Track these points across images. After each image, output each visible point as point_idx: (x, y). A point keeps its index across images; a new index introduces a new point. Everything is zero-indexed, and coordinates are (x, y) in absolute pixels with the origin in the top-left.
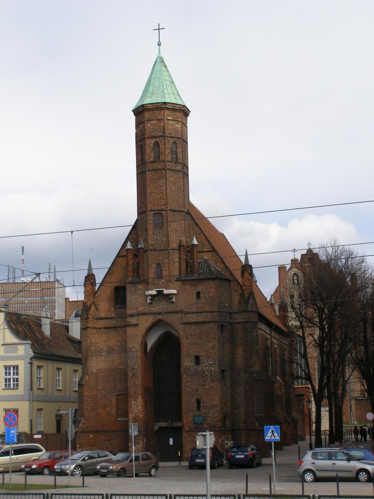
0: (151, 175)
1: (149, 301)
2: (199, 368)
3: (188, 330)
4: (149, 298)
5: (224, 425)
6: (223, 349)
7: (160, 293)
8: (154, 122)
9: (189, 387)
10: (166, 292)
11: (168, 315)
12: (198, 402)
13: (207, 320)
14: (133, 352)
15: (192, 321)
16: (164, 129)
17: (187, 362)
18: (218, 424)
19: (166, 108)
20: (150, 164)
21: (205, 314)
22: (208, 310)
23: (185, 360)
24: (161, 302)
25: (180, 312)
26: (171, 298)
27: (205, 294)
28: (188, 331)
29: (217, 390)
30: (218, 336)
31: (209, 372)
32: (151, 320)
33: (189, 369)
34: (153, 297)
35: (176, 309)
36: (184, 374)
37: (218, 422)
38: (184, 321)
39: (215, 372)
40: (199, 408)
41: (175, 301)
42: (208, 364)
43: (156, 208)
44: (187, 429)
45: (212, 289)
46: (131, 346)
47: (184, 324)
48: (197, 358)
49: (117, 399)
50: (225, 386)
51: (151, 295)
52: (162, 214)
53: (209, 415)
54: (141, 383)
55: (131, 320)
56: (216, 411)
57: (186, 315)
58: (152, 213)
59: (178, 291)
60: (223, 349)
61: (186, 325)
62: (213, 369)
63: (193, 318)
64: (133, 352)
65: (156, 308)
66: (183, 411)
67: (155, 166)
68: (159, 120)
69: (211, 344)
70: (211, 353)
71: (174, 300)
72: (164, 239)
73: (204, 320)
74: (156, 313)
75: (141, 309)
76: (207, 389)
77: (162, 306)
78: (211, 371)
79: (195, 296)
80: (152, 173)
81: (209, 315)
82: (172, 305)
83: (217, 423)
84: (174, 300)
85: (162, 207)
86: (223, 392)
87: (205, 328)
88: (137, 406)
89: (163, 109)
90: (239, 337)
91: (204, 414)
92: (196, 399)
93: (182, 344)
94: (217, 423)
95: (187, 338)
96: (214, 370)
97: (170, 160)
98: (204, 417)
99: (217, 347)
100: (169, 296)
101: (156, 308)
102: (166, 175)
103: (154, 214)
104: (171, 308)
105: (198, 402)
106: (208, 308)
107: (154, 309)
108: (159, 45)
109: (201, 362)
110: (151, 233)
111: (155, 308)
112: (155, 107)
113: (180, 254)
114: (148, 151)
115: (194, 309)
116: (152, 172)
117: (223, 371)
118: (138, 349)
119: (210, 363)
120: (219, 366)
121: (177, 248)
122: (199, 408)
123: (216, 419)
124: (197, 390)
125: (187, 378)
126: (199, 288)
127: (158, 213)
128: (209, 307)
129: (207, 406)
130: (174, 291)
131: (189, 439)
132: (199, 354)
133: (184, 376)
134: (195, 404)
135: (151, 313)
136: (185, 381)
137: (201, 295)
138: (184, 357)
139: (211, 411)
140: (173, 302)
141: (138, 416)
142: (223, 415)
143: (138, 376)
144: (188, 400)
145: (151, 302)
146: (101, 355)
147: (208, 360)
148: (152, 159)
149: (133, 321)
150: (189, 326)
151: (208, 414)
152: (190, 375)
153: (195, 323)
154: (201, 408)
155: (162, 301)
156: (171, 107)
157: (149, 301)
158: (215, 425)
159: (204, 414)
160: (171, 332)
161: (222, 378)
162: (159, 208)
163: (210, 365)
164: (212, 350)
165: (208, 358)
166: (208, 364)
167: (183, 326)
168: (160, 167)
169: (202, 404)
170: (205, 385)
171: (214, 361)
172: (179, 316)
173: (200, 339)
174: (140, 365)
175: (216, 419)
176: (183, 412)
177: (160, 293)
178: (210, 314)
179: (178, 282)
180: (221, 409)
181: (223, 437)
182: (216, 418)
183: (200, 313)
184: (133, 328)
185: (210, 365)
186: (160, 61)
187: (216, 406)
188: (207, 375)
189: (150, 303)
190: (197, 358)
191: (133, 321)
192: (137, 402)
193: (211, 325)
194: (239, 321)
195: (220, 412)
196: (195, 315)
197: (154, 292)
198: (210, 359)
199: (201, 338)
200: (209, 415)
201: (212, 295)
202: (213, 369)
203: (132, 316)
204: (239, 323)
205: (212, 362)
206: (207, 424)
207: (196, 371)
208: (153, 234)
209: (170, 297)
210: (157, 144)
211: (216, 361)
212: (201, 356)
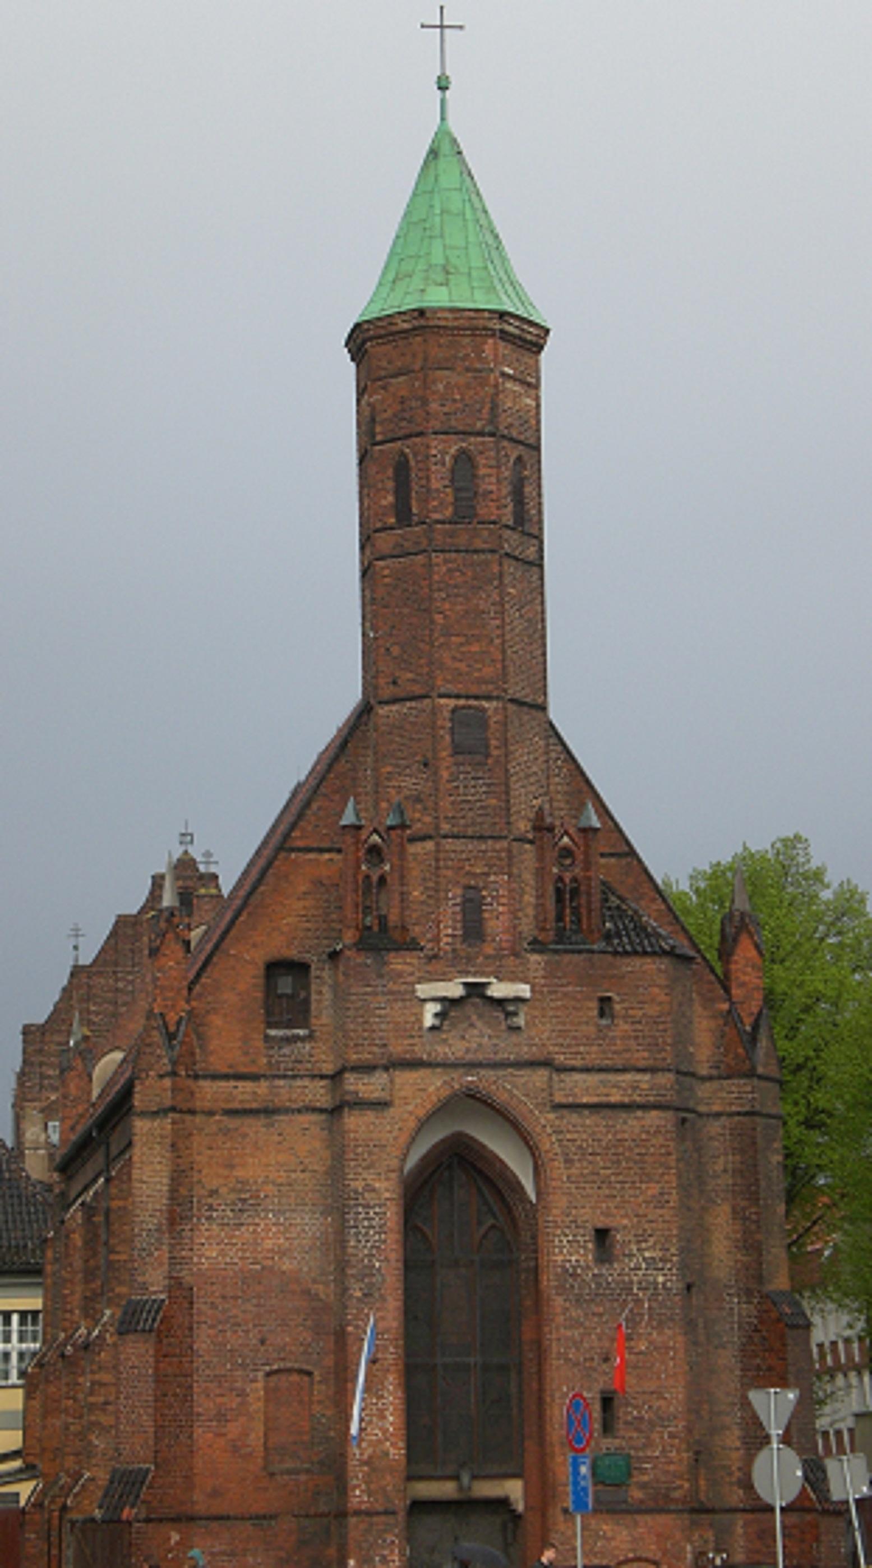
0: (444, 569)
2: (611, 1273)
3: (569, 1131)
7: (475, 990)
10: (498, 990)
16: (494, 407)
17: (566, 1251)
18: (681, 1487)
23: (561, 1241)
28: (569, 1136)
31: (646, 1289)
32: (435, 1085)
33: (574, 1275)
34: (449, 1003)
36: (558, 1294)
37: (681, 1478)
38: (559, 1098)
41: (527, 1023)
42: (644, 1259)
45: (656, 990)
46: (359, 1185)
49: (266, 1389)
51: (442, 1000)
56: (672, 1436)
57: (562, 1076)
61: (565, 1112)
62: (661, 1279)
69: (654, 1189)
70: (652, 1221)
71: (520, 1021)
74: (454, 1066)
76: (641, 1353)
77: (477, 1038)
80: (450, 562)
82: (514, 1038)
83: (678, 1482)
84: (520, 1021)
87: (632, 1124)
89: (493, 335)
90: (719, 1167)
94: (678, 1482)
96: (664, 1284)
102: (501, 575)
104: (509, 1048)
105: (607, 1402)
106: (641, 1057)
107: (447, 1050)
108: (443, 88)
109: (617, 1250)
111: (450, 1046)
115: (593, 1055)
116: (447, 555)
119: (647, 1254)
121: (530, 836)
123: (672, 1468)
125: (567, 1309)
130: (524, 990)
135: (438, 1065)
138: (559, 1232)
140: (519, 1028)
145: (437, 1022)
146: (209, 1218)
147: (644, 1245)
150: (574, 1118)
151: (645, 1446)
156: (517, 332)
160: (472, 1138)
165: (641, 1238)
166: (644, 1259)
167: (551, 1116)
172: (540, 1077)
175: (672, 1468)
177: (475, 990)
180: (689, 1430)
182: (672, 1462)
185: (650, 1262)
193: (654, 1118)
194: (716, 1108)
196: (592, 1079)
197: (455, 989)
202: (661, 1279)
204: (718, 1115)
205: (657, 1254)
206: (643, 1486)
207: (599, 1285)
210: (465, 459)
211: (673, 1250)
212: (617, 1230)
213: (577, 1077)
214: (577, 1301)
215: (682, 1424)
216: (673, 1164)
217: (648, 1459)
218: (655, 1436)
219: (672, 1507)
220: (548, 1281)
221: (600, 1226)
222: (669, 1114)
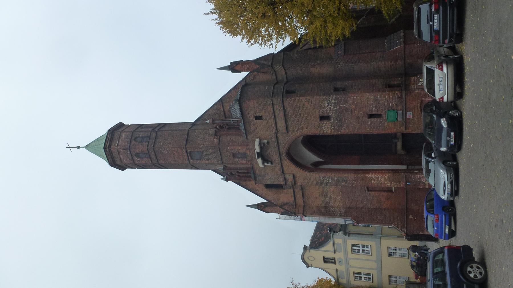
1: (270, 165)
2: (333, 116)
4: (266, 164)
5: (398, 86)
6: (311, 91)
7: (260, 155)
8: (121, 156)
9: (354, 126)
11: (280, 146)
12: (371, 116)
13: (282, 108)
14: (321, 180)
15: (284, 124)
17: (327, 129)
19: (108, 148)
20: (153, 161)
21: (276, 111)
22: (271, 109)
24: (269, 153)
25: (276, 135)
26: (264, 144)
27: (256, 111)
29: (356, 97)
30: (297, 96)
33: (334, 126)
35: (274, 139)
38: (284, 130)
39: (336, 99)
40: (379, 116)
43: (186, 157)
44: (403, 128)
47: (288, 131)
48: (323, 118)
50: (352, 87)
52: (190, 153)
53: (386, 104)
54: (352, 174)
55: (290, 181)
58: (191, 161)
59: (257, 138)
60: (311, 91)
62: (333, 101)
63: (281, 123)
64: (321, 180)
65: (276, 158)
66: (381, 132)
67: (153, 157)
68: (119, 153)
71: (265, 141)
72: (211, 150)
73: (282, 112)
75: (279, 172)
77: (272, 152)
78: (335, 103)
79: (260, 121)
81: (276, 107)
84: (265, 141)
85: (185, 152)
86: (360, 89)
87: (289, 110)
88: (378, 178)
91: (385, 109)
92: (368, 118)
93: (309, 133)
95: (302, 128)
97: (147, 143)
98: (388, 110)
99: (308, 97)
100: (262, 147)
101: (276, 158)
103: (192, 159)
105: (371, 116)
109: (326, 115)
110: (207, 162)
112: (110, 156)
113: (223, 135)
114: (144, 162)
115: (272, 122)
117: (336, 90)
118: (317, 176)
120: (329, 95)
122: (379, 116)
124: (358, 118)
126: (251, 118)
127: (190, 155)
128: (269, 107)
129: (376, 107)
130: (257, 141)
131: (416, 126)
132: (318, 116)
133: (342, 131)
134: (373, 120)
136: (347, 131)
137: (258, 115)
139: (381, 102)
140: (268, 143)
141: (388, 177)
142: (386, 88)
143: (345, 177)
144: (370, 127)
147: (323, 107)
148: (149, 159)
149: (290, 178)
150: (290, 127)
152: (341, 126)
153: (286, 121)
154: (378, 113)
155: (268, 152)
157: (270, 165)
158: (399, 97)
159: (385, 109)
161: (344, 90)
162: (186, 154)
163: (329, 104)
164: (313, 102)
167: (290, 133)
168: (153, 153)
169: (374, 113)
170: (352, 110)
171: (324, 100)
172: (280, 137)
173: (302, 115)
174: (333, 174)
176: (383, 132)
177: (260, 155)
178: (275, 106)
179: (249, 137)
181: (413, 87)
182: (389, 97)
183: (275, 116)
184: (297, 179)
185: (329, 104)
186: (87, 147)
187: (375, 96)
188: (340, 108)
189: (272, 163)
190: (323, 118)
191: (290, 178)
192: (373, 178)
193: (286, 104)
195: (383, 91)
198: (322, 104)
199: (300, 114)
200: (386, 104)
201: (256, 105)
202: (333, 101)
203: (285, 179)
205: (326, 102)
207: (337, 119)
208: (208, 160)
209: (262, 145)
210: (137, 155)
213: (278, 126)
214: (341, 126)
215: (377, 94)
216: (298, 98)
217: (389, 104)
218: (381, 102)
219: (404, 97)
220: (336, 133)
221: (319, 120)
222: (285, 99)
